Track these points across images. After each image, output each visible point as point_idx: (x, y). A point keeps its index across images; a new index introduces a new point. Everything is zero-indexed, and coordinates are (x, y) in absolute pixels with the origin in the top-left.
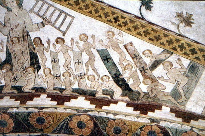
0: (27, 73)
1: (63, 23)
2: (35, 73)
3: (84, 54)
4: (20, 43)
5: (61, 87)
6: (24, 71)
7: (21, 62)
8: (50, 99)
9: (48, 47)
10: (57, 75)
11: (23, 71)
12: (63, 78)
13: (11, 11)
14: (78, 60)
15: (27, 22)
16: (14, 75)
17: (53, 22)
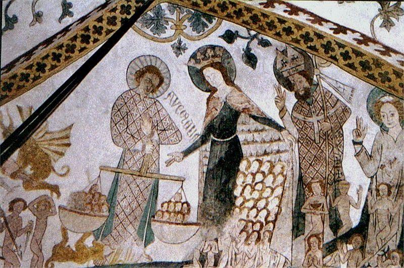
0: (389, 261)
4: (390, 198)
7: (384, 238)
13: (388, 131)
16: (366, 259)
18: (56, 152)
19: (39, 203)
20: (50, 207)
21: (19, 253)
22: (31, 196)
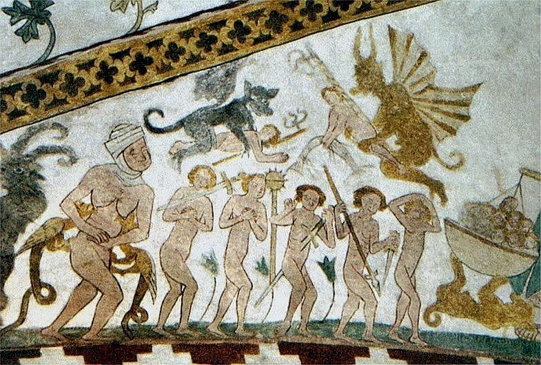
18: (442, 125)
19: (409, 204)
20: (429, 217)
21: (375, 282)
22: (394, 188)
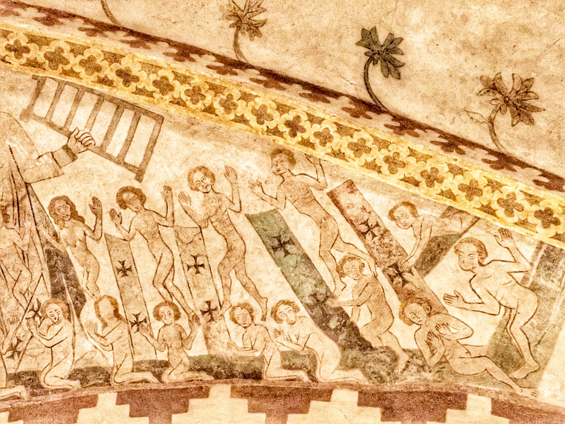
0: (47, 322)
1: (129, 141)
2: (69, 319)
3: (209, 232)
4: (11, 225)
5: (153, 357)
6: (37, 319)
7: (25, 289)
8: (126, 408)
9: (98, 226)
10: (137, 316)
11: (34, 317)
12: (157, 325)
14: (195, 258)
15: (22, 154)
16: (11, 334)
17: (99, 141)
